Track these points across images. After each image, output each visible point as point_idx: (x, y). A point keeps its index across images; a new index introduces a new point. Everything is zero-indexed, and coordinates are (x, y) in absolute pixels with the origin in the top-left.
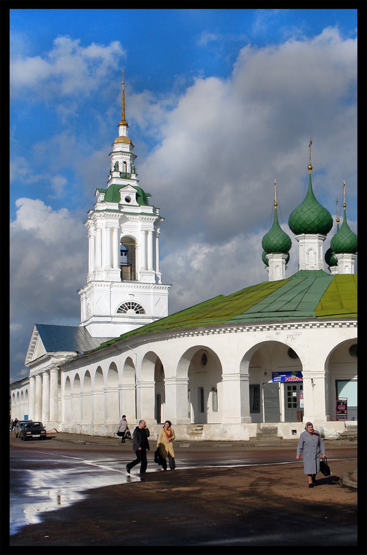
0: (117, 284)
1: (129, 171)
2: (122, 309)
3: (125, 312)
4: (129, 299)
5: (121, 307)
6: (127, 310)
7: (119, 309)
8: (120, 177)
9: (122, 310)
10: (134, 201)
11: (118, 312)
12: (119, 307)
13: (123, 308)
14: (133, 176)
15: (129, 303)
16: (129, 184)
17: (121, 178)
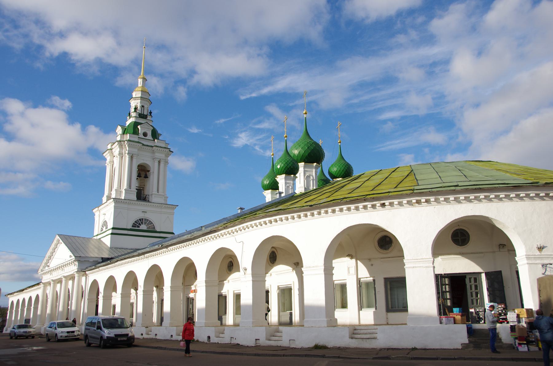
0: (134, 202)
1: (145, 113)
2: (137, 224)
3: (138, 227)
4: (141, 216)
5: (136, 222)
6: (140, 225)
7: (134, 224)
8: (138, 117)
9: (136, 225)
10: (149, 137)
11: (133, 226)
12: (134, 222)
13: (137, 223)
14: (149, 118)
15: (143, 219)
16: (147, 122)
17: (140, 117)
